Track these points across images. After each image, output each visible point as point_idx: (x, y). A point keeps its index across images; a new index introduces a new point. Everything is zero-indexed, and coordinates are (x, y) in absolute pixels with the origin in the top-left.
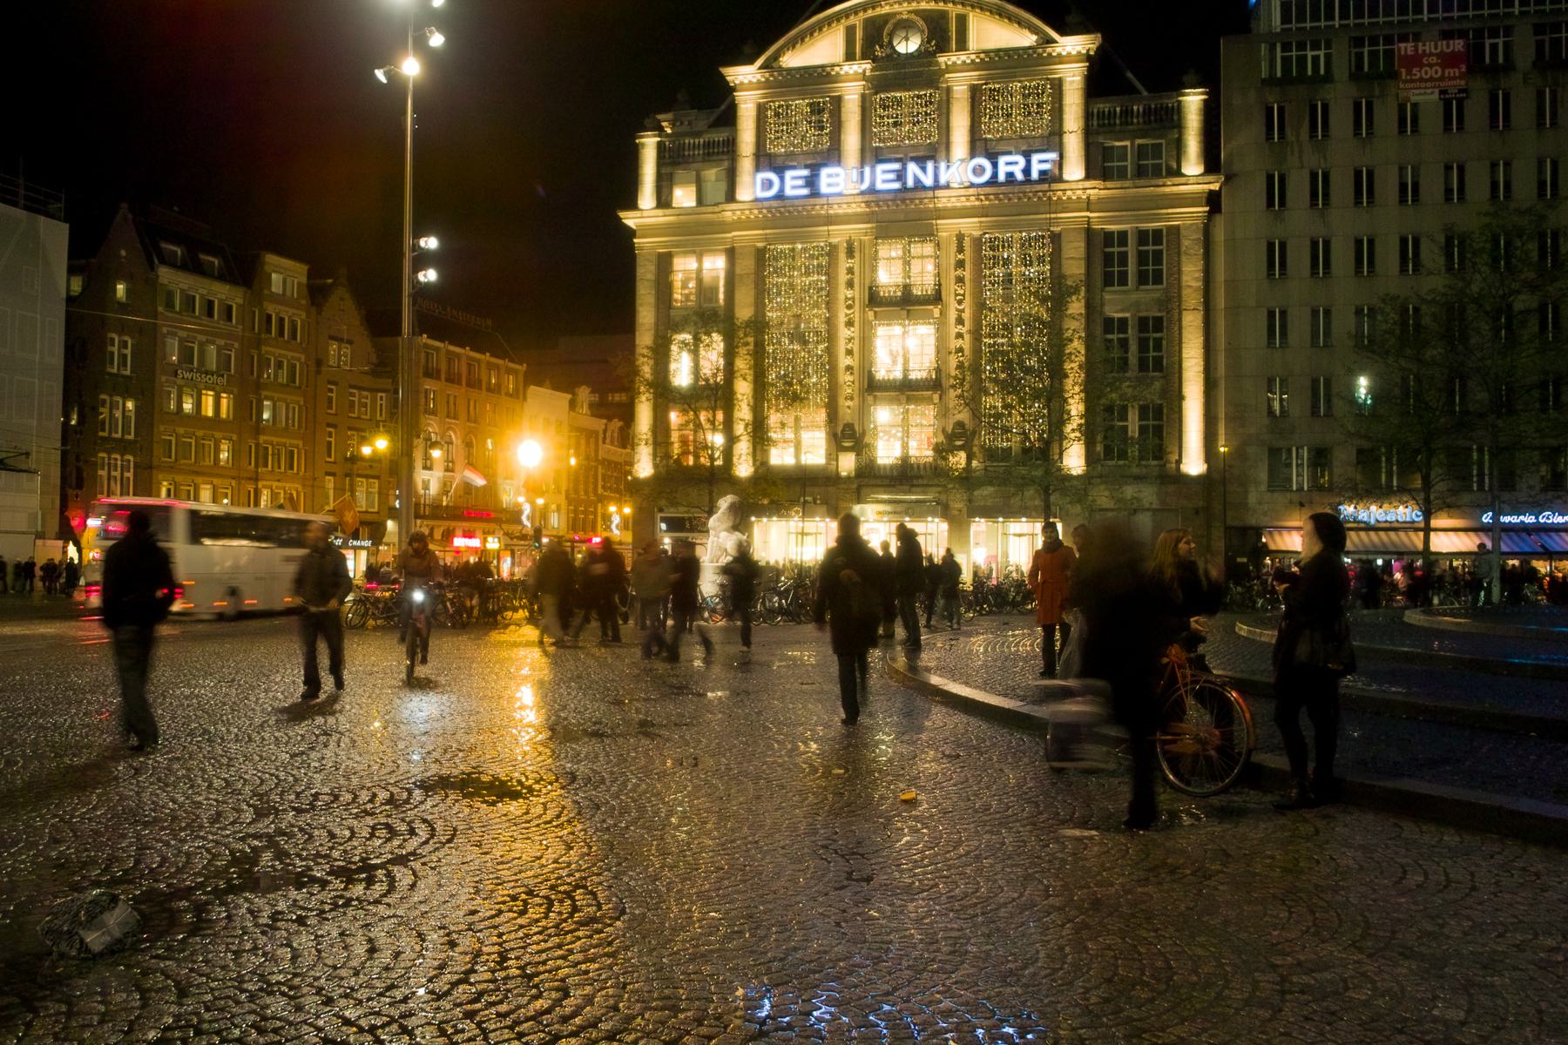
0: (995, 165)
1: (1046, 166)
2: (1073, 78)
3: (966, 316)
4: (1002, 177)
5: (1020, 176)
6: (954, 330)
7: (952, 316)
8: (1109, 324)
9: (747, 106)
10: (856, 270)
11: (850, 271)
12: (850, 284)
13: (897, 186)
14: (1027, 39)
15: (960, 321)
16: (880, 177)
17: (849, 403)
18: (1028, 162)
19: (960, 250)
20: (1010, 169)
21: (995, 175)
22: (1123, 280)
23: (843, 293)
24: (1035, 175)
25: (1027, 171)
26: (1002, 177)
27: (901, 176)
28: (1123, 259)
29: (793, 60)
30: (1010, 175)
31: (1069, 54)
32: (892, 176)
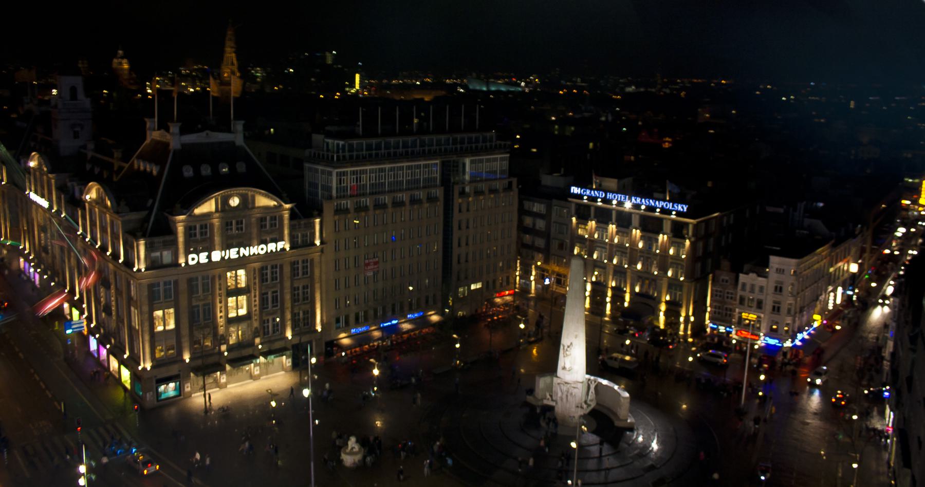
2: (286, 215)
3: (257, 293)
5: (274, 250)
6: (253, 299)
7: (253, 295)
8: (295, 288)
9: (180, 229)
10: (222, 283)
11: (220, 285)
12: (220, 289)
14: (273, 203)
15: (255, 296)
17: (222, 328)
19: (255, 273)
23: (218, 292)
24: (278, 250)
25: (276, 248)
27: (238, 253)
29: (198, 211)
30: (272, 251)
31: (286, 208)
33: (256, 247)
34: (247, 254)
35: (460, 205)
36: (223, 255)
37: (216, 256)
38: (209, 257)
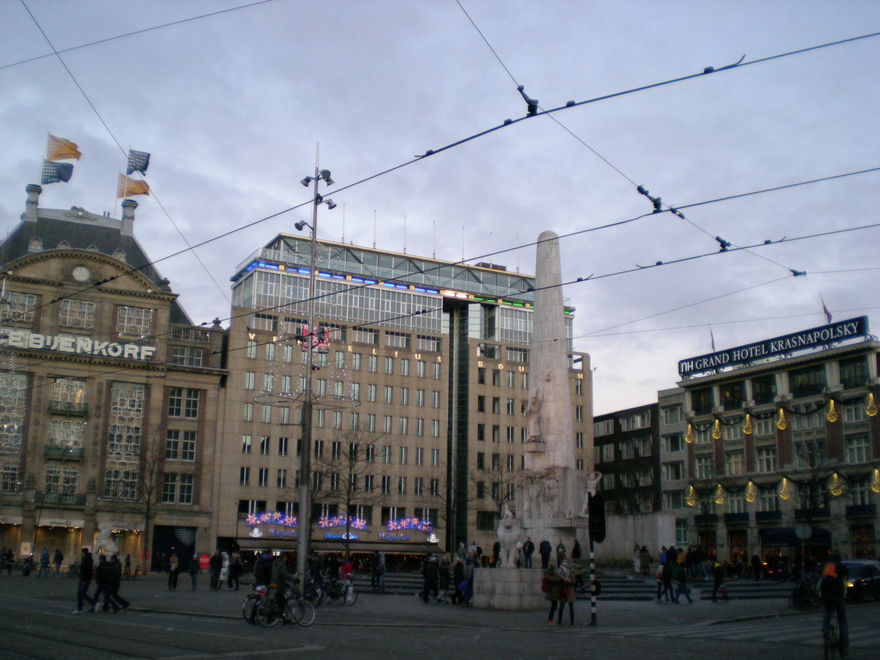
0: (123, 348)
1: (150, 354)
4: (126, 356)
5: (135, 357)
8: (170, 433)
13: (72, 350)
18: (140, 350)
20: (131, 351)
21: (123, 353)
22: (178, 413)
24: (143, 357)
25: (139, 354)
26: (126, 356)
27: (74, 345)
28: (179, 404)
32: (70, 345)
33: (106, 344)
34: (88, 350)
35: (481, 370)
36: (48, 343)
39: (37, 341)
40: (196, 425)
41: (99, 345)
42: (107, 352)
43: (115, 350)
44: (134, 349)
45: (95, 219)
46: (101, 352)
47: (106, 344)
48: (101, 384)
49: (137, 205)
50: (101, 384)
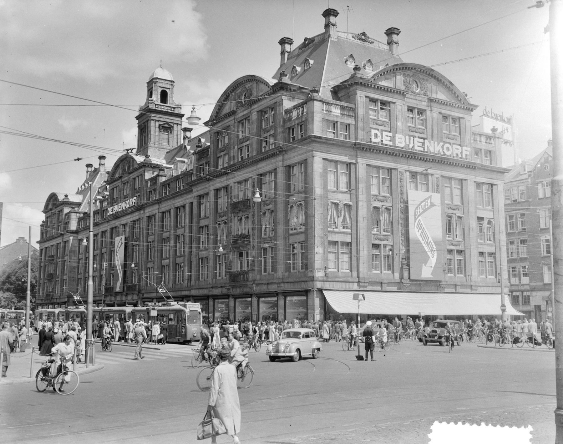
1: (468, 153)
4: (455, 155)
16: (416, 144)
24: (464, 156)
25: (461, 153)
30: (457, 154)
33: (442, 144)
37: (401, 142)
38: (393, 139)
39: (400, 140)
40: (492, 213)
41: (438, 144)
42: (444, 152)
43: (448, 149)
44: (458, 149)
45: (373, 43)
46: (439, 151)
47: (442, 144)
48: (437, 178)
49: (400, 32)
50: (437, 178)
